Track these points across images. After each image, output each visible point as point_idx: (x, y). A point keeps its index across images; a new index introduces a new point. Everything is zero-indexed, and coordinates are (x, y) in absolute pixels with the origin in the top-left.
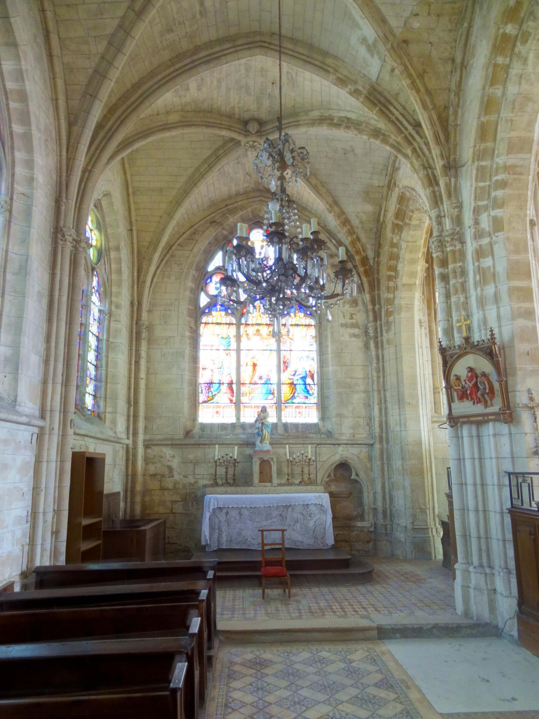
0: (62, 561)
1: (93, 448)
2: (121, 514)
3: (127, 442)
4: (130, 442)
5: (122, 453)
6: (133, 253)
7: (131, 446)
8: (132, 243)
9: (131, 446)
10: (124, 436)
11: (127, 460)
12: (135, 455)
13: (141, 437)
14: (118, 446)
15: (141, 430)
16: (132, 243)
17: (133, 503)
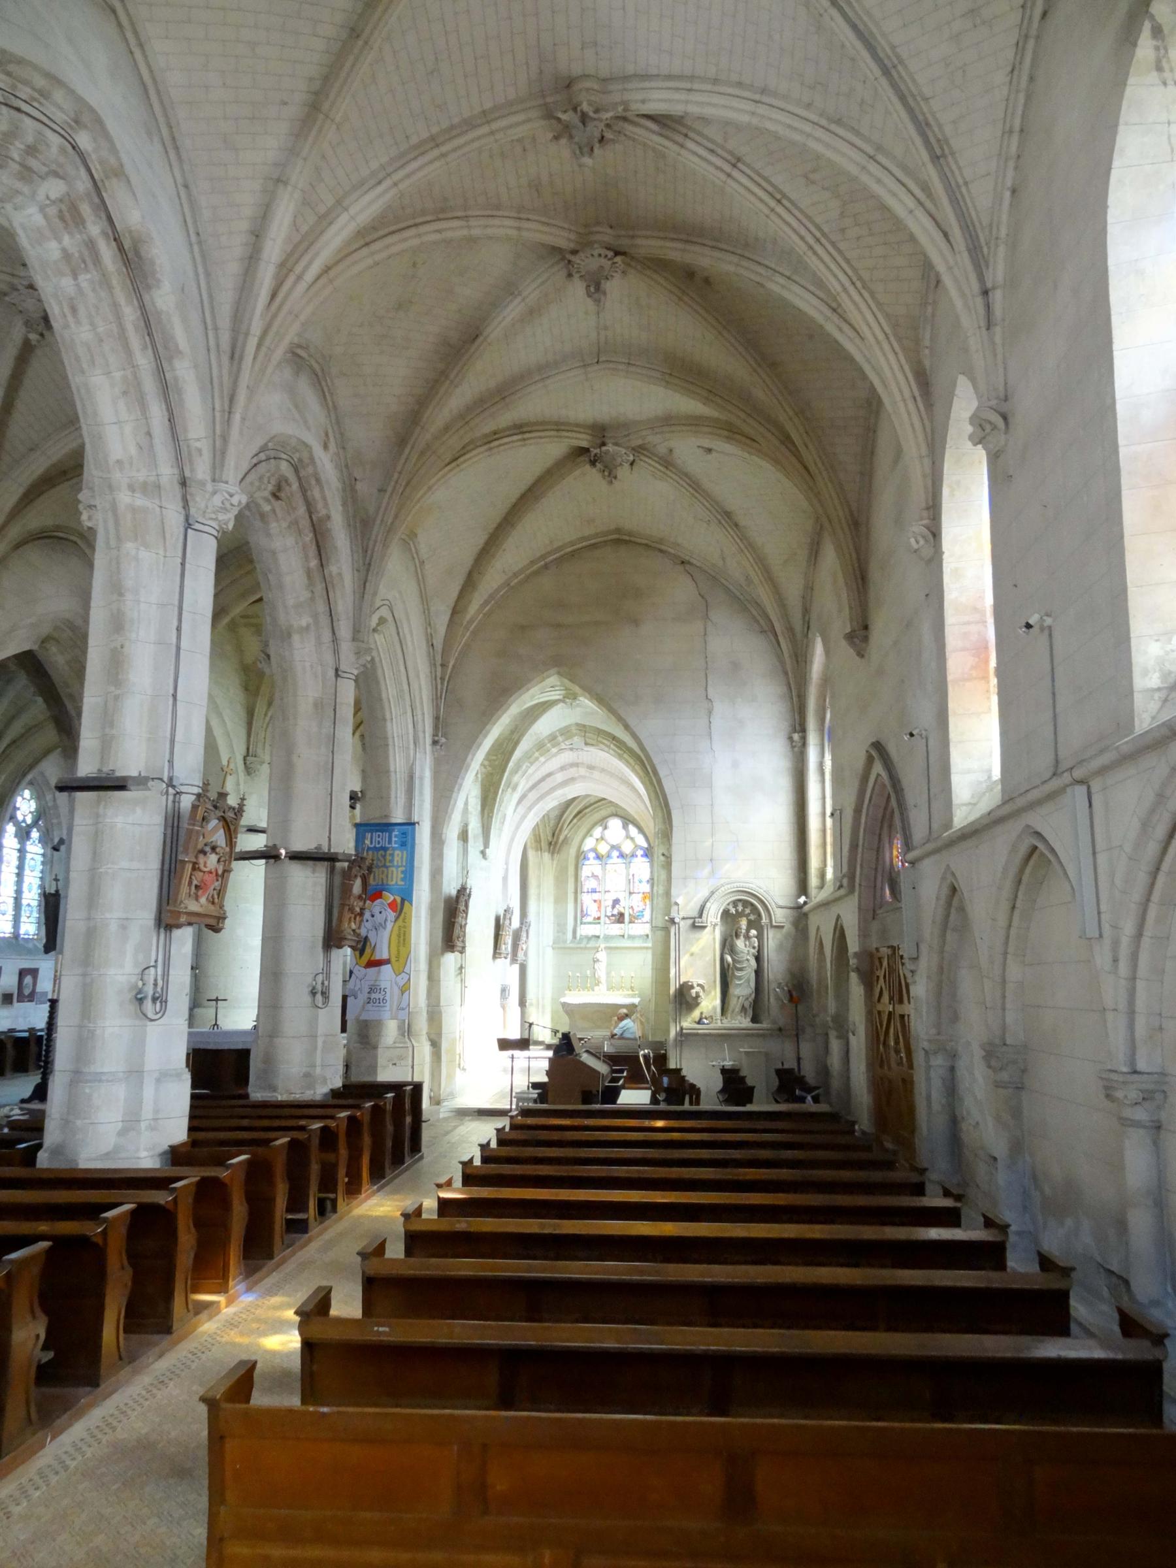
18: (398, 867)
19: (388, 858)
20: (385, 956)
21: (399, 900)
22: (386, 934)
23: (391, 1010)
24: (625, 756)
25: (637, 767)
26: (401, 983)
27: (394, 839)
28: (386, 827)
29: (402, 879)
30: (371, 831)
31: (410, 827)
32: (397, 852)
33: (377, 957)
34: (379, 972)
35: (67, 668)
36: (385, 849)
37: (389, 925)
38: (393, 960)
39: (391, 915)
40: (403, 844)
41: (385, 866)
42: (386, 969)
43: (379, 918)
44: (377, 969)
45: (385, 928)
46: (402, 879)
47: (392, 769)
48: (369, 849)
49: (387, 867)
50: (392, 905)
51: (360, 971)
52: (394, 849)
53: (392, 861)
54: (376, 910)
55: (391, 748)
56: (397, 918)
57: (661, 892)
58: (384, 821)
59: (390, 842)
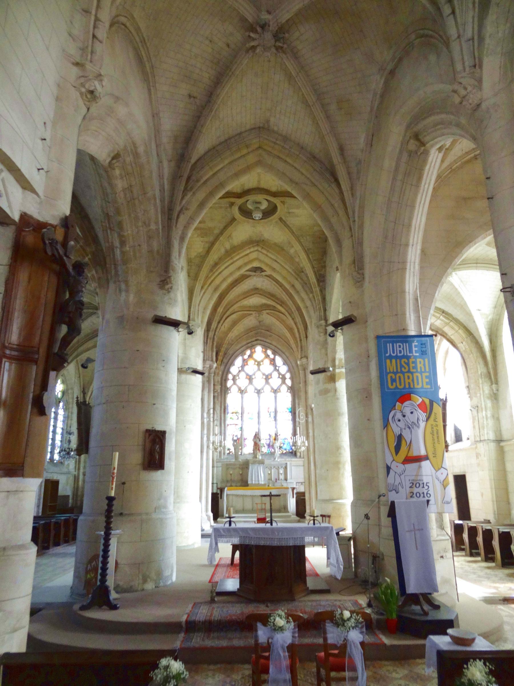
0: (40, 514)
1: (55, 477)
2: (70, 505)
3: (74, 473)
4: (76, 473)
5: (72, 479)
6: (80, 386)
7: (76, 475)
8: (80, 382)
9: (76, 475)
10: (74, 470)
11: (75, 481)
12: (78, 479)
13: (82, 471)
14: (69, 475)
15: (81, 468)
16: (80, 382)
17: (76, 500)
18: (421, 373)
19: (411, 365)
20: (423, 452)
21: (427, 402)
22: (420, 432)
23: (436, 503)
24: (451, 323)
25: (460, 331)
26: (442, 478)
27: (414, 349)
28: (406, 339)
29: (427, 383)
30: (393, 343)
31: (428, 339)
32: (418, 360)
33: (414, 453)
34: (420, 467)
35: (122, 195)
36: (408, 358)
37: (422, 424)
38: (431, 456)
39: (422, 416)
40: (423, 353)
41: (409, 371)
42: (426, 465)
43: (412, 418)
44: (415, 465)
45: (418, 427)
46: (427, 383)
47: (407, 290)
48: (391, 357)
49: (412, 373)
50: (422, 406)
51: (397, 467)
52: (415, 357)
53: (415, 367)
54: (407, 411)
55: (408, 270)
56: (428, 419)
57: (489, 415)
58: (403, 334)
59: (411, 351)
